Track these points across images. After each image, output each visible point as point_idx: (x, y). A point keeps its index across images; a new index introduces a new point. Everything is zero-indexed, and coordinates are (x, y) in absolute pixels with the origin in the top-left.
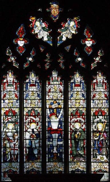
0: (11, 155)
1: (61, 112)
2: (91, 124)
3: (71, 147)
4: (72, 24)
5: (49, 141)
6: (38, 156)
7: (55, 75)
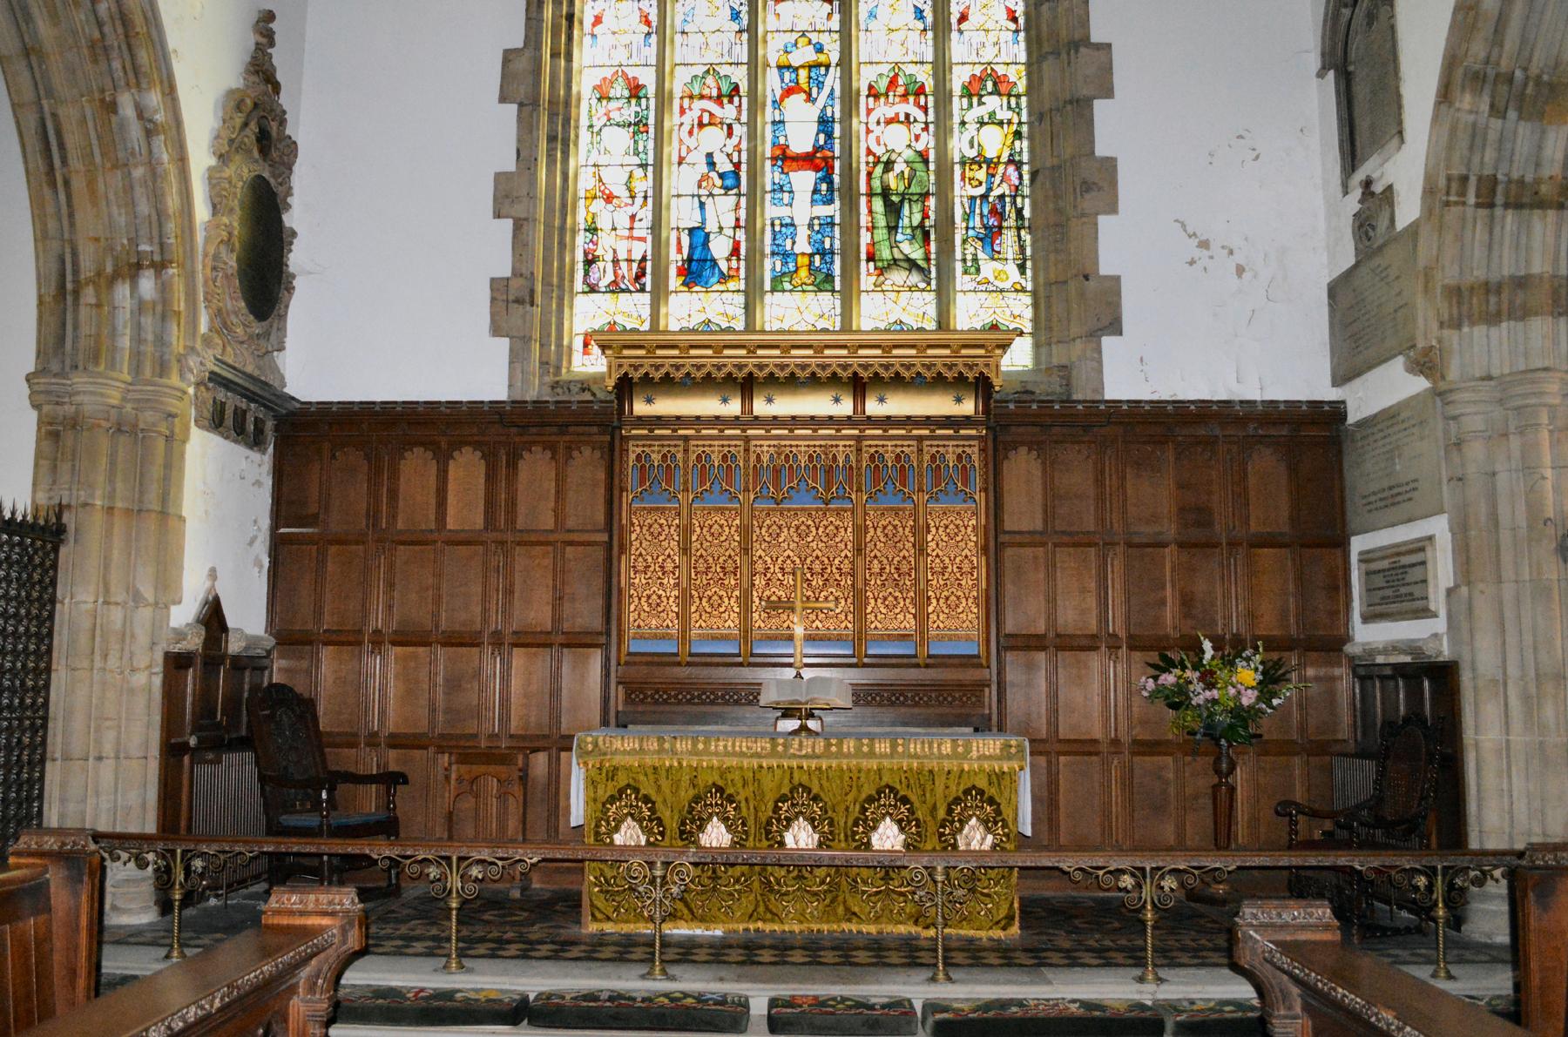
0: (616, 262)
1: (829, 82)
2: (952, 130)
3: (872, 229)
5: (777, 202)
6: (730, 268)
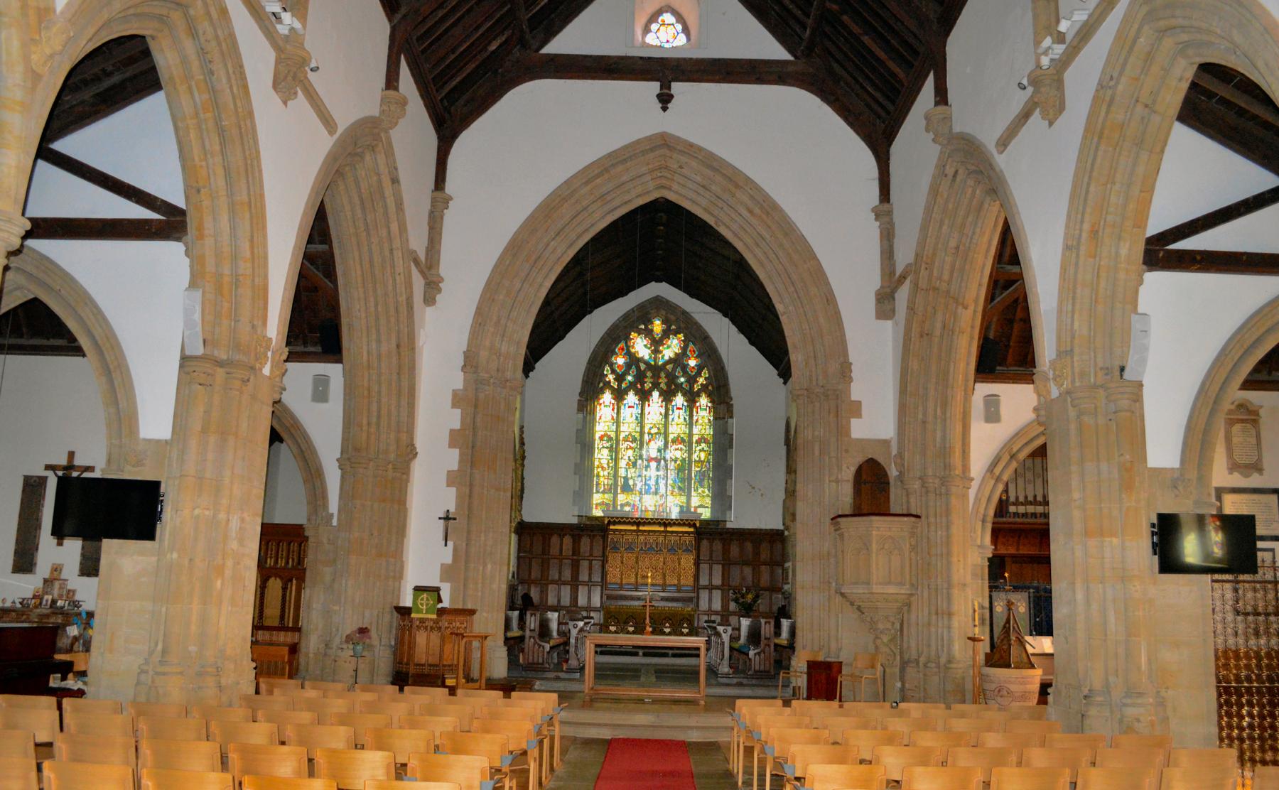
4: (675, 341)
7: (656, 394)
